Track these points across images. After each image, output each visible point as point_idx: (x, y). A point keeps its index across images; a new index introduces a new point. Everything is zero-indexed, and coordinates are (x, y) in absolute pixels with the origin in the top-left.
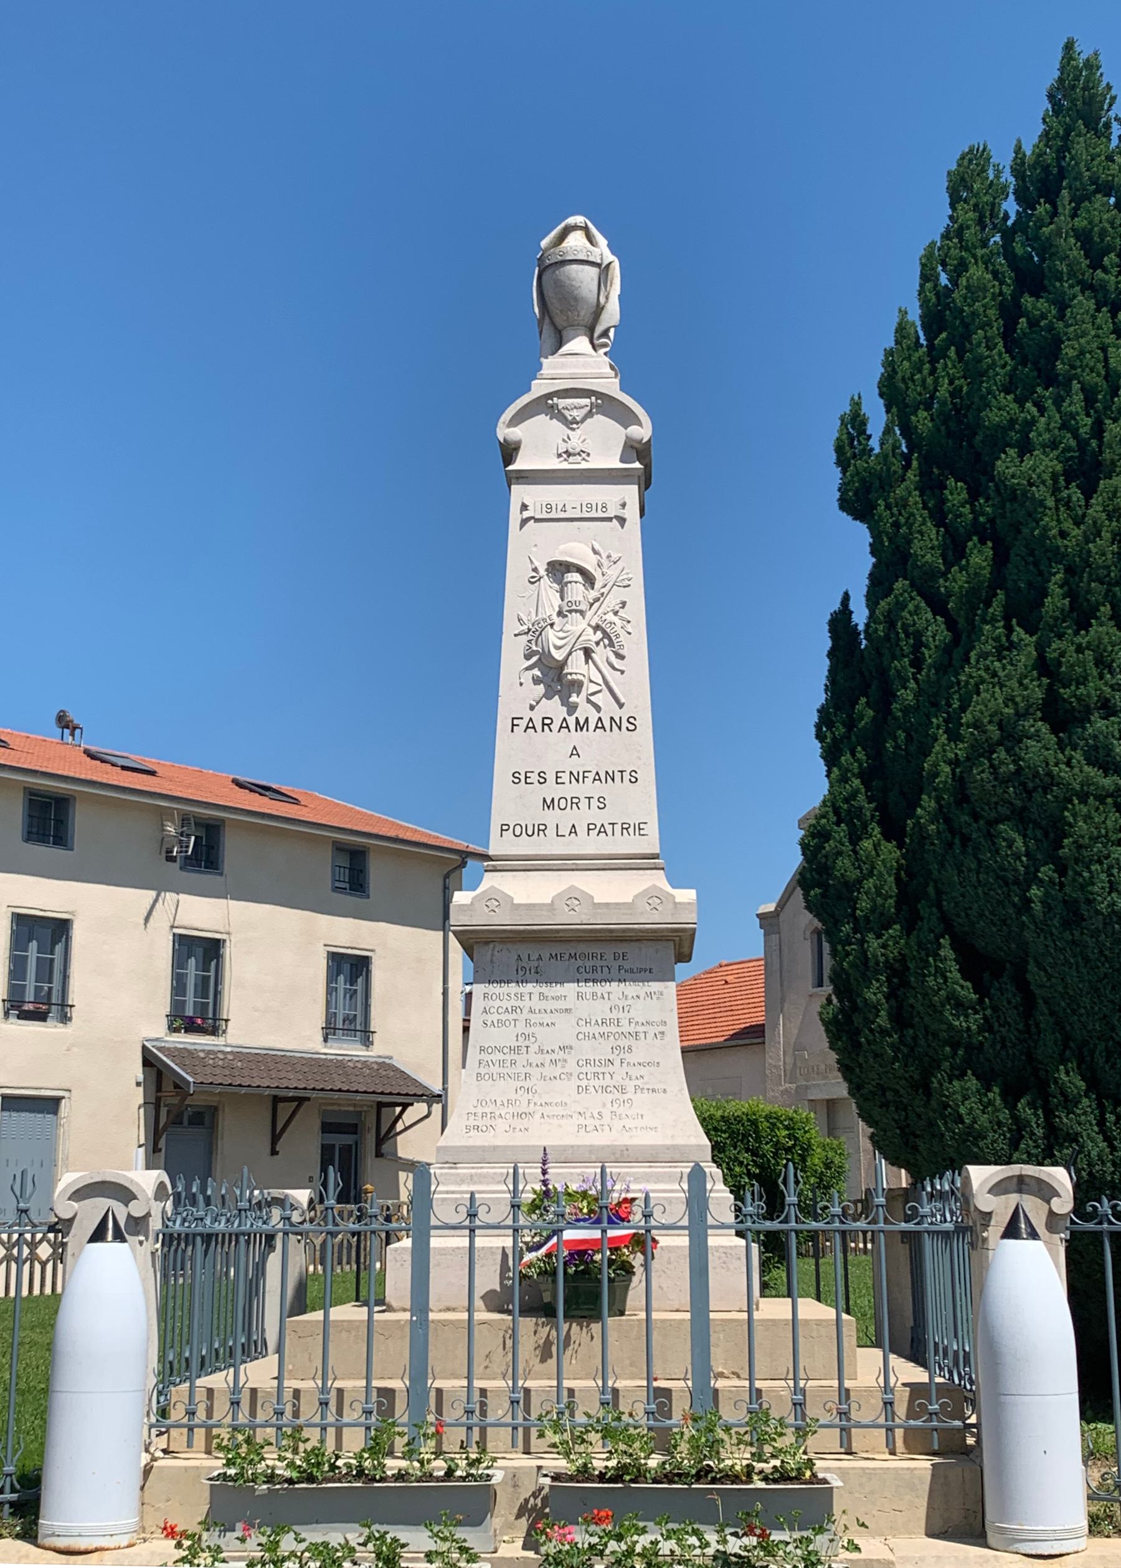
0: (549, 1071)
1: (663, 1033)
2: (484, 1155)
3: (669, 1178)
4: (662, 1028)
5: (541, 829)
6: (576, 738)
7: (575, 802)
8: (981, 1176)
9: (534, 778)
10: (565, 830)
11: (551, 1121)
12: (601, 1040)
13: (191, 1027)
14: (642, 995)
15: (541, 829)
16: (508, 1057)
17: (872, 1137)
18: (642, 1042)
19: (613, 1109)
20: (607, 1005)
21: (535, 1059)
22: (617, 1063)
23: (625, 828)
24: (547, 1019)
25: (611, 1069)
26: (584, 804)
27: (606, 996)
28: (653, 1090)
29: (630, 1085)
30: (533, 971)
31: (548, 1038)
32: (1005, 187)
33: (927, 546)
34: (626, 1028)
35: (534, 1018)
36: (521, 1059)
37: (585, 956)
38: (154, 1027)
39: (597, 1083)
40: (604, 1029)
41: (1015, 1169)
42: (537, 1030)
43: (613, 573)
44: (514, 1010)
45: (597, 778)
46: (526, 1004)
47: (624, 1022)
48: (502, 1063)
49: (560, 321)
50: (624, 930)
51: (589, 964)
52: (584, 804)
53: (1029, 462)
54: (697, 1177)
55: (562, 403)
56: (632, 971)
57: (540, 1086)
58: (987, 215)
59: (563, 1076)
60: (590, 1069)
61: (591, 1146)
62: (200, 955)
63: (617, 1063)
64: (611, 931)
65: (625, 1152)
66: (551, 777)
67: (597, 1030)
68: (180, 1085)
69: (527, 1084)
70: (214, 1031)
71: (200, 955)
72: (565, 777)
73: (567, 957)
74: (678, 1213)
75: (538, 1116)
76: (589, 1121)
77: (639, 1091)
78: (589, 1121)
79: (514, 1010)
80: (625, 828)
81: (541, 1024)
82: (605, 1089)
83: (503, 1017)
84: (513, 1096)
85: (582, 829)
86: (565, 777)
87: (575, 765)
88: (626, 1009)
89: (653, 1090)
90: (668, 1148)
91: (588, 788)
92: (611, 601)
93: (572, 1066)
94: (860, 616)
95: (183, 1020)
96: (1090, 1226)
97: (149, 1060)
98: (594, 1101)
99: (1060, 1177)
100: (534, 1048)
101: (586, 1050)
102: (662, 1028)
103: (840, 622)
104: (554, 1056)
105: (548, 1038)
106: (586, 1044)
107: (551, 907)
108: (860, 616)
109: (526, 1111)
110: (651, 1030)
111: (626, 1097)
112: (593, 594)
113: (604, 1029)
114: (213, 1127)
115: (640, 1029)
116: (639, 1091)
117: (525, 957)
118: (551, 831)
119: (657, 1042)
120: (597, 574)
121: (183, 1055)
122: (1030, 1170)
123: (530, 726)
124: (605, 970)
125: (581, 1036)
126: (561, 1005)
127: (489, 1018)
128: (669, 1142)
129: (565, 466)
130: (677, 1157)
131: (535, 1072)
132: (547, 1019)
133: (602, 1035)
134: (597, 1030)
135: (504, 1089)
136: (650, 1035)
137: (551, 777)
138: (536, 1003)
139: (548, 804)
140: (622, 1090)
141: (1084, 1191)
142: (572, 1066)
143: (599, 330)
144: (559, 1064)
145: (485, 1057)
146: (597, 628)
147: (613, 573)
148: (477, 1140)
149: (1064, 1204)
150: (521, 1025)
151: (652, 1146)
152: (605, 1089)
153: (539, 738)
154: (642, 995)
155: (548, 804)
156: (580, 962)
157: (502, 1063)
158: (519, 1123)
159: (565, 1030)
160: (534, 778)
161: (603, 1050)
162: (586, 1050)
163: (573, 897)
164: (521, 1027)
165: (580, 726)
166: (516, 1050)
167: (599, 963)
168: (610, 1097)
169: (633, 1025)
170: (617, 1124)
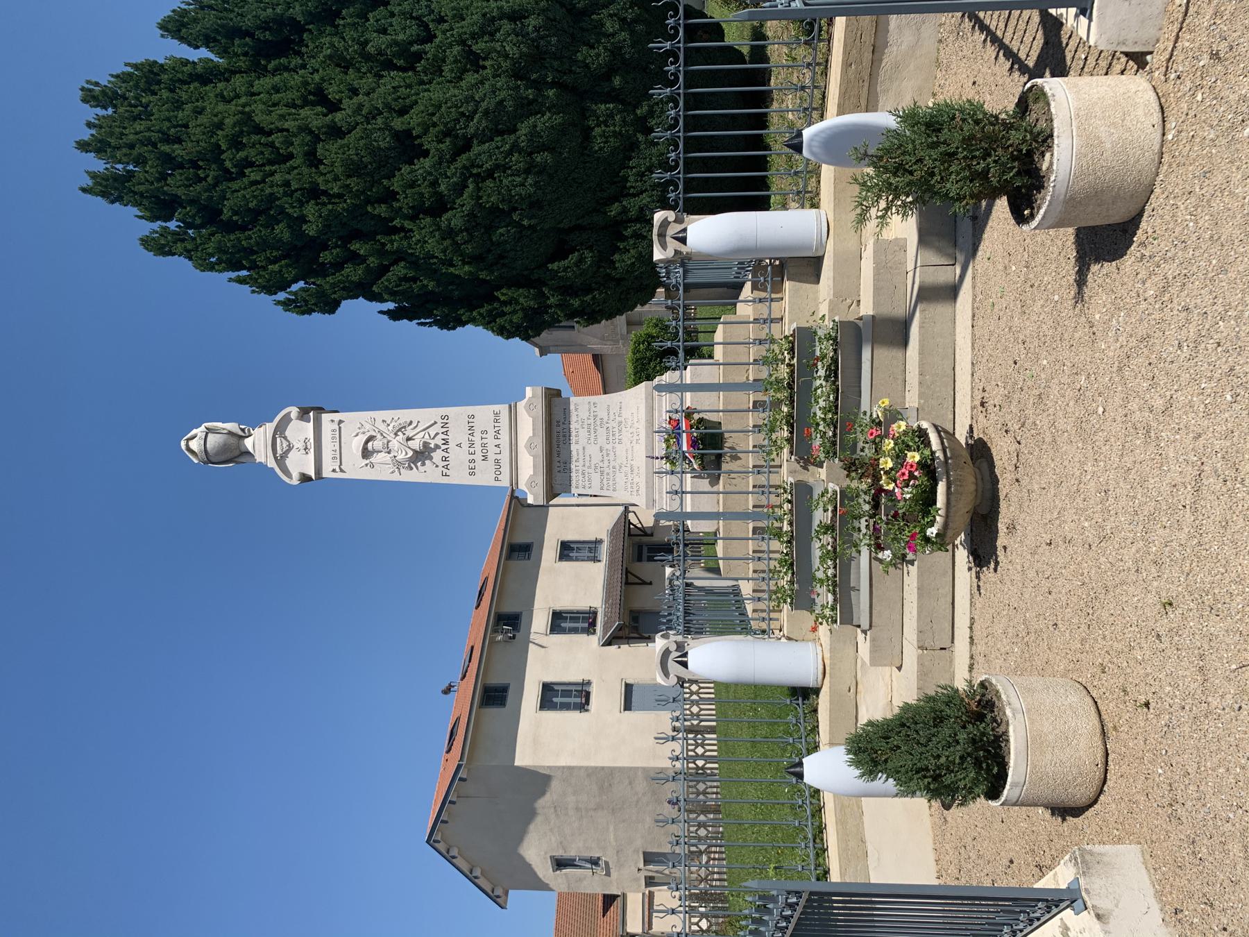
0: (612, 457)
2: (650, 486)
3: (660, 401)
5: (497, 462)
6: (452, 445)
7: (484, 446)
8: (658, 255)
9: (472, 465)
10: (498, 450)
13: (593, 624)
15: (497, 462)
17: (642, 305)
23: (496, 421)
24: (587, 458)
26: (485, 441)
29: (618, 419)
31: (597, 457)
32: (162, 227)
33: (353, 273)
35: (587, 464)
36: (606, 470)
37: (558, 441)
38: (594, 641)
41: (655, 238)
42: (593, 462)
43: (368, 427)
45: (472, 435)
46: (580, 468)
48: (608, 480)
49: (237, 453)
52: (485, 441)
53: (311, 218)
54: (659, 388)
55: (279, 452)
57: (619, 461)
58: (179, 237)
62: (561, 621)
66: (472, 457)
67: (593, 435)
68: (620, 628)
70: (595, 613)
71: (561, 621)
72: (472, 450)
74: (675, 397)
76: (635, 437)
78: (635, 437)
80: (496, 421)
85: (497, 442)
86: (472, 450)
87: (465, 445)
91: (477, 439)
92: (382, 427)
93: (609, 447)
94: (391, 305)
95: (590, 629)
96: (681, 203)
97: (608, 643)
98: (626, 436)
99: (658, 216)
101: (602, 440)
103: (394, 315)
106: (599, 440)
107: (535, 457)
108: (391, 305)
110: (593, 409)
112: (379, 436)
114: (639, 612)
118: (498, 457)
120: (368, 434)
121: (605, 630)
122: (655, 231)
123: (446, 467)
129: (312, 450)
131: (612, 464)
132: (587, 458)
134: (593, 435)
135: (620, 478)
137: (472, 457)
139: (485, 458)
141: (665, 206)
142: (609, 447)
143: (241, 433)
146: (396, 434)
147: (368, 427)
148: (643, 490)
149: (671, 215)
150: (591, 471)
153: (452, 463)
155: (485, 458)
157: (608, 480)
158: (636, 471)
159: (593, 450)
160: (472, 465)
161: (602, 432)
162: (602, 440)
163: (530, 446)
164: (591, 471)
165: (446, 442)
170: (636, 425)
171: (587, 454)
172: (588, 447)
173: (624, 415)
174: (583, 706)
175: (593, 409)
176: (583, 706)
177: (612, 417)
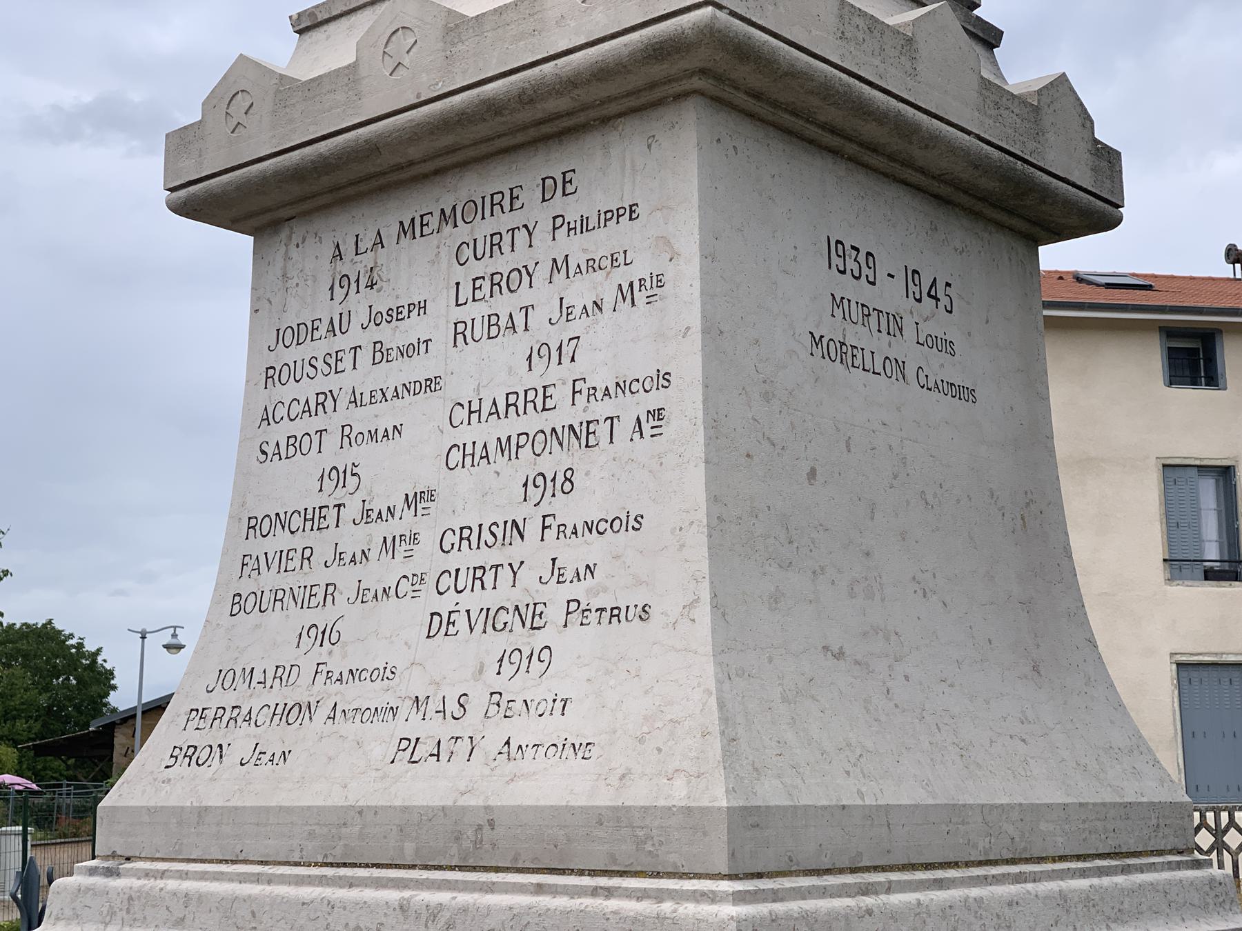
1: (657, 414)
4: (654, 400)
11: (351, 728)
12: (501, 461)
14: (609, 299)
16: (298, 542)
18: (603, 452)
19: (498, 684)
20: (519, 344)
21: (352, 538)
22: (532, 530)
25: (518, 550)
27: (519, 320)
28: (615, 614)
30: (363, 281)
31: (387, 473)
34: (565, 414)
37: (477, 209)
39: (474, 600)
40: (510, 426)
42: (363, 454)
44: (324, 400)
47: (561, 395)
50: (526, 98)
51: (483, 229)
56: (585, 225)
59: (405, 586)
60: (466, 558)
61: (405, 809)
63: (532, 530)
64: (492, 108)
65: (486, 829)
69: (321, 617)
73: (434, 221)
75: (323, 712)
77: (575, 618)
78: (433, 729)
79: (324, 400)
81: (372, 435)
82: (491, 619)
83: (298, 428)
84: (287, 656)
88: (567, 351)
89: (615, 614)
90: (600, 818)
98: (459, 663)
100: (353, 510)
102: (654, 400)
104: (393, 527)
105: (387, 473)
109: (304, 700)
110: (631, 408)
111: (540, 639)
113: (510, 426)
115: (601, 409)
116: (575, 618)
117: (348, 248)
119: (645, 445)
124: (521, 236)
125: (456, 456)
126: (417, 369)
127: (279, 433)
128: (605, 798)
130: (626, 853)
132: (383, 414)
133: (503, 445)
136: (624, 428)
138: (367, 377)
140: (531, 616)
144: (401, 550)
145: (258, 546)
150: (331, 441)
151: (556, 811)
152: (491, 619)
154: (609, 299)
156: (463, 232)
164: (333, 454)
166: (314, 519)
167: (504, 221)
168: (498, 643)
169: (581, 399)
171: (411, 411)
172: (434, 406)
173: (574, 646)
174: (1178, 565)
175: (631, 408)
176: (1178, 565)
177: (573, 554)
